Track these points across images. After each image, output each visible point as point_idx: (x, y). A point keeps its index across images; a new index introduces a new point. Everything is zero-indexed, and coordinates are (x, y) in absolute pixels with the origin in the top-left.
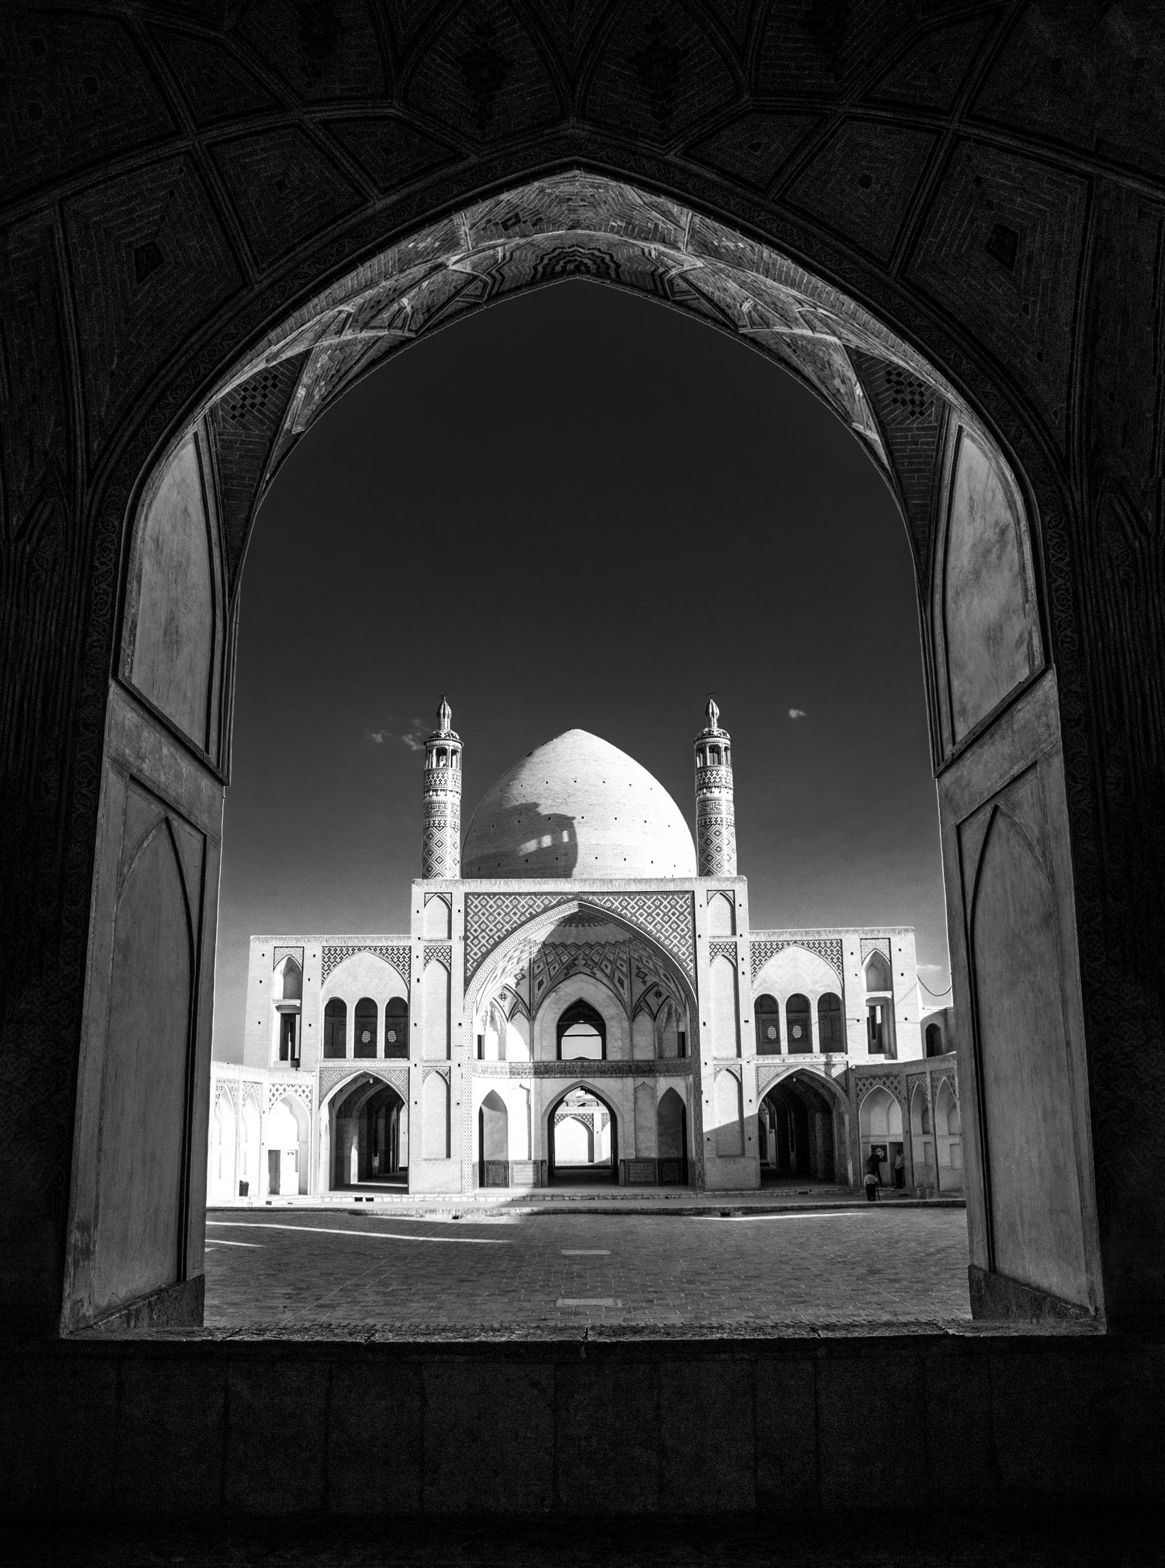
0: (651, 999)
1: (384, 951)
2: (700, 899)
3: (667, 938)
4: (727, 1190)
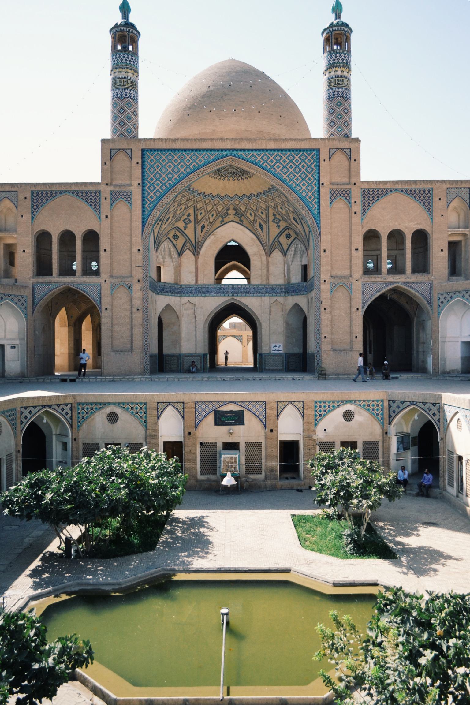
0: (283, 240)
1: (80, 194)
2: (324, 155)
3: (298, 185)
4: (338, 374)
